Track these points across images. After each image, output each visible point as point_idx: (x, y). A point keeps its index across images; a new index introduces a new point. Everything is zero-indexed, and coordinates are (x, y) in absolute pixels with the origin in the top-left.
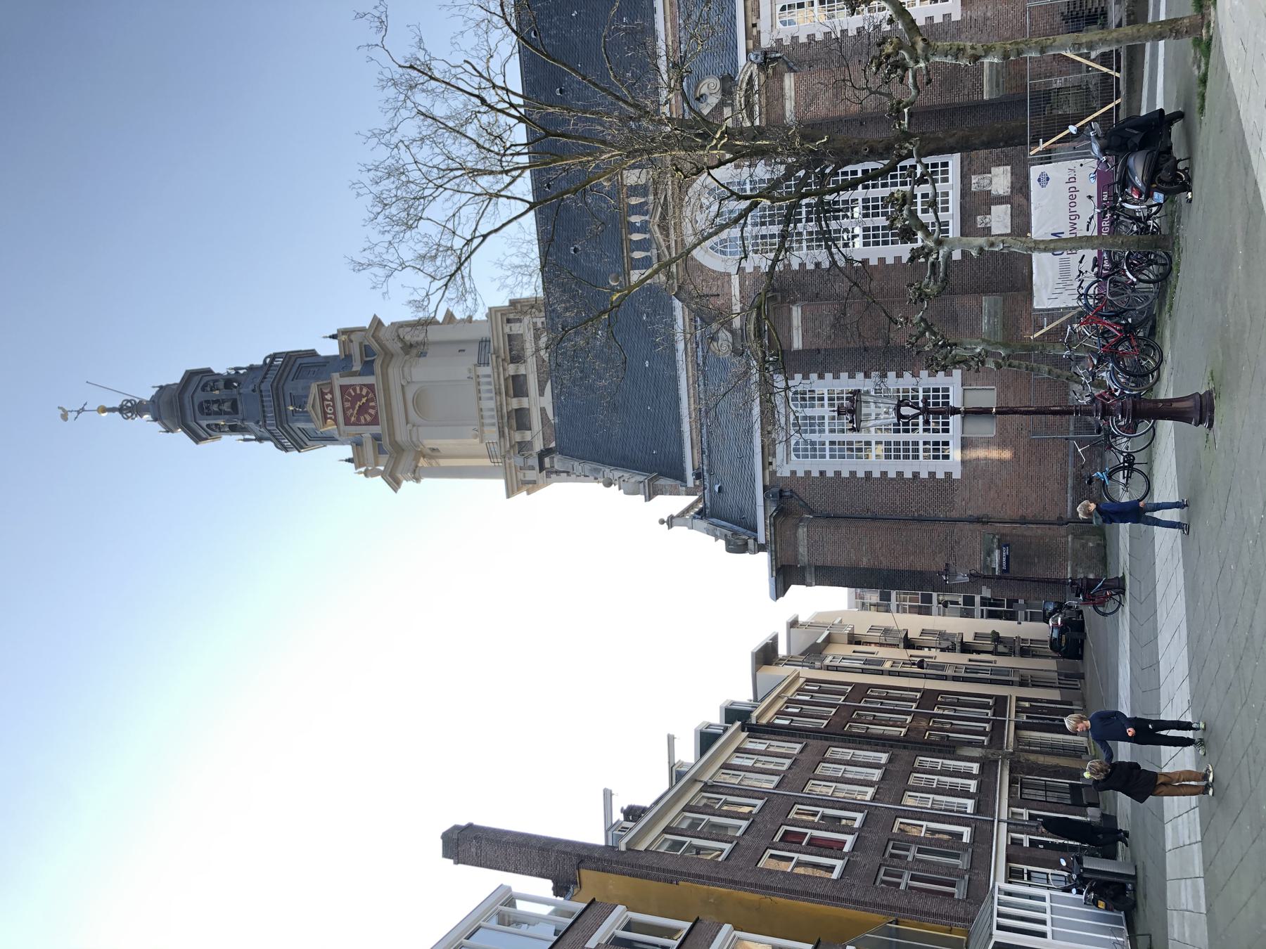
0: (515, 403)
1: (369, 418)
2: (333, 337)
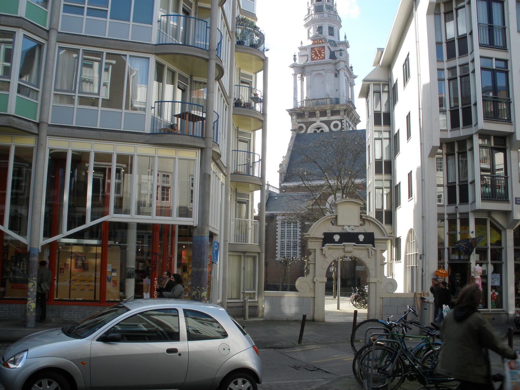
0: (318, 112)
1: (313, 57)
2: (345, 37)
